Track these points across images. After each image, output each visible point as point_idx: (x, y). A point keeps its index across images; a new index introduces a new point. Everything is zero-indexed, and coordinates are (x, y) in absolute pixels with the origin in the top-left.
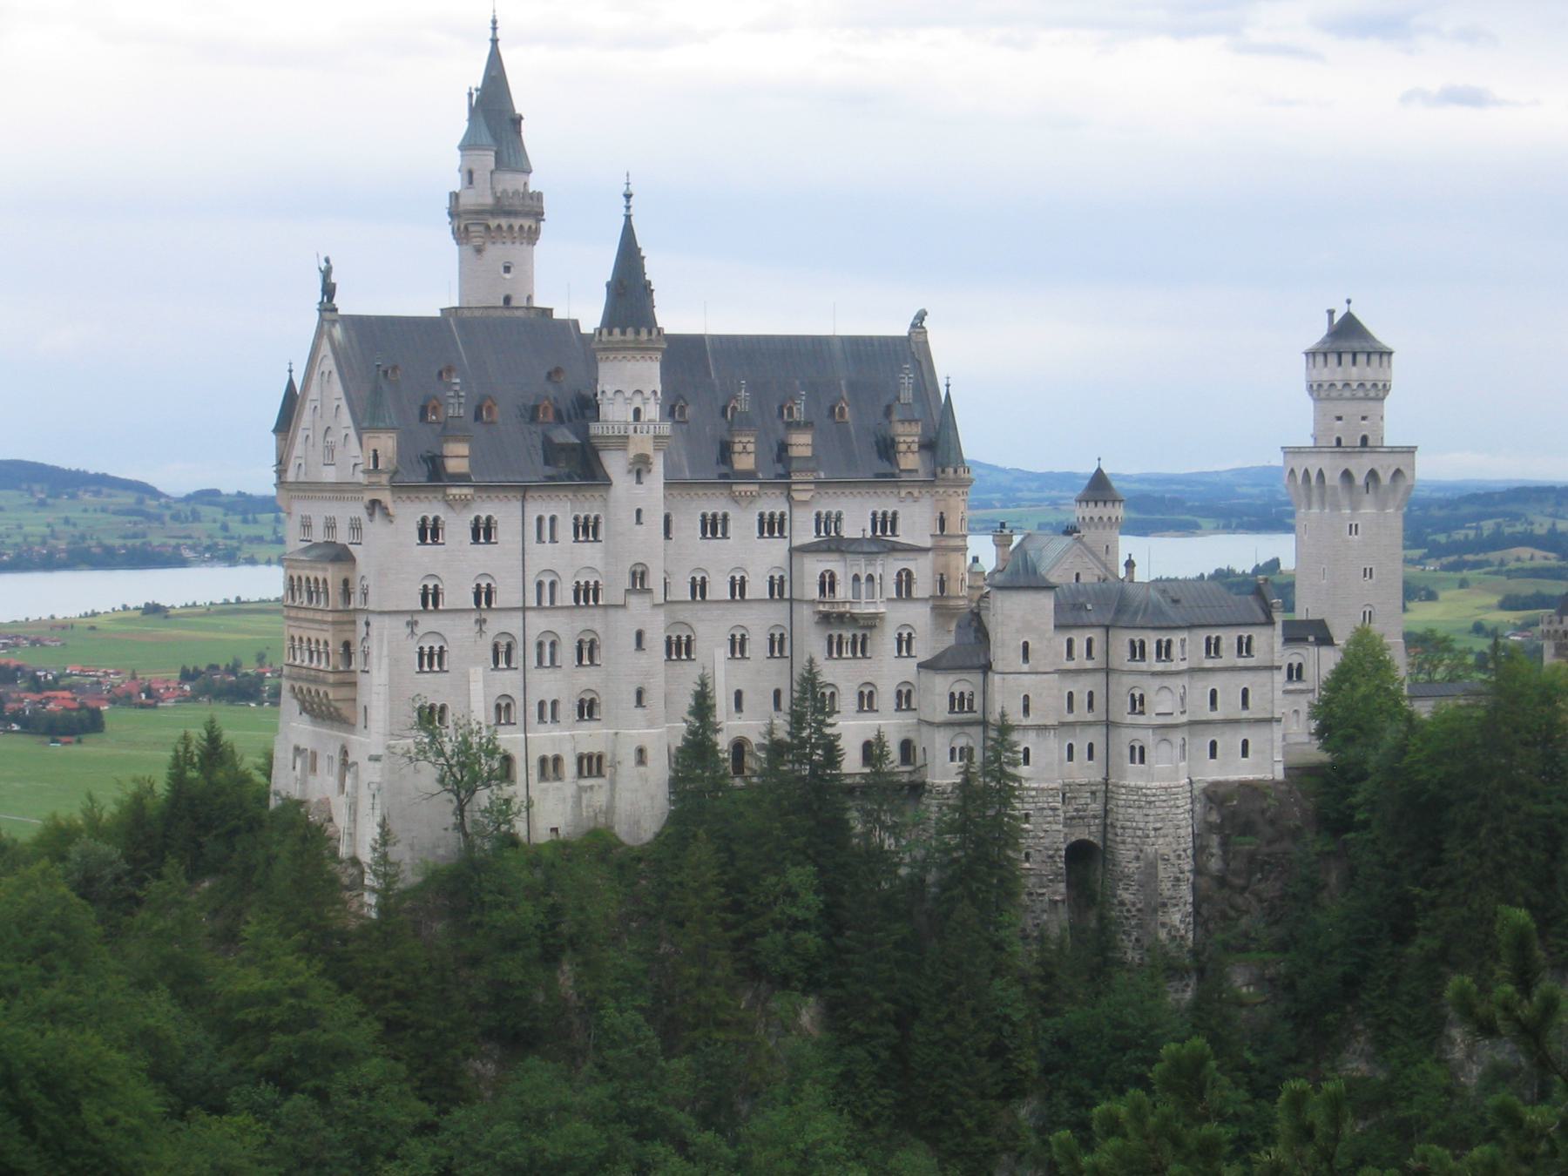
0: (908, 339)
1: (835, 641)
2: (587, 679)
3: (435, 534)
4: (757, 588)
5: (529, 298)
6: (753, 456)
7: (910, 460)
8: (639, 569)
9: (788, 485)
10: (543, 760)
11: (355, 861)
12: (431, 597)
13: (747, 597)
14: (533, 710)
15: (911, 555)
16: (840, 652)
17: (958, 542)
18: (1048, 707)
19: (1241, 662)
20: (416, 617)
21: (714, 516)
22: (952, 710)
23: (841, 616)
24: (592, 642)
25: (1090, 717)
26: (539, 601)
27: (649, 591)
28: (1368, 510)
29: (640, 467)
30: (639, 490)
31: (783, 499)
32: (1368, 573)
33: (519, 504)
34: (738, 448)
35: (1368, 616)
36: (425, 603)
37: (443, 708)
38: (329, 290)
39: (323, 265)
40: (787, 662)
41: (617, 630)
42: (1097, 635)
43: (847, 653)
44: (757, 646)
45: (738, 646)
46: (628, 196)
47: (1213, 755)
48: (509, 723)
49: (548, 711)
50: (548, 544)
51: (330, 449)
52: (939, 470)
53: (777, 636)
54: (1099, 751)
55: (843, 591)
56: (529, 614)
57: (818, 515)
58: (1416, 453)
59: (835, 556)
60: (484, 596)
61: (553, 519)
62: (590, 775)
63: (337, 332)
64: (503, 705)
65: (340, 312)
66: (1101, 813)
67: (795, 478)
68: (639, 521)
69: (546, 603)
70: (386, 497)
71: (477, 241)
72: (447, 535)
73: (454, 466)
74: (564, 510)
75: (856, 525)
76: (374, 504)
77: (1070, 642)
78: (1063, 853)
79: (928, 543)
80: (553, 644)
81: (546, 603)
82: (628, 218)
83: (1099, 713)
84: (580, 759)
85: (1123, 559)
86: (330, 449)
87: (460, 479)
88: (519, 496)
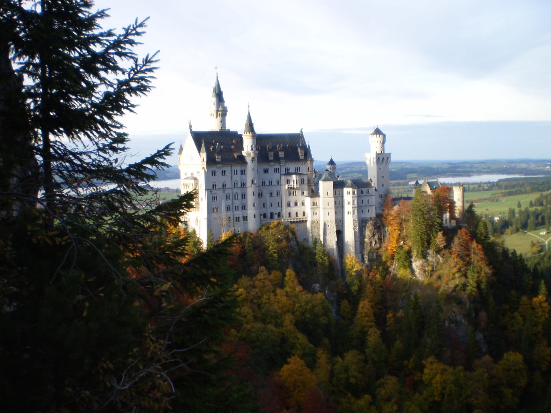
0: (299, 134)
1: (290, 192)
2: (244, 201)
3: (215, 175)
4: (274, 183)
5: (226, 128)
6: (273, 157)
7: (302, 157)
8: (253, 180)
9: (280, 163)
10: (236, 218)
11: (201, 239)
12: (214, 186)
13: (273, 184)
14: (234, 208)
15: (304, 175)
16: (291, 195)
17: (312, 173)
18: (332, 204)
19: (367, 194)
20: (212, 190)
21: (266, 169)
22: (313, 205)
23: (291, 188)
24: (244, 194)
25: (339, 206)
26: (235, 187)
27: (256, 184)
28: (383, 165)
29: (253, 159)
30: (253, 164)
31: (279, 165)
32: (383, 177)
33: (230, 167)
34: (270, 155)
35: (383, 185)
36: (213, 187)
37: (217, 208)
38: (191, 126)
39: (189, 122)
40: (280, 197)
41: (250, 191)
42: (340, 190)
43: (292, 195)
44: (275, 194)
45: (271, 194)
46: (249, 107)
47: (363, 212)
48: (229, 211)
49: (237, 208)
50: (236, 175)
51: (191, 159)
52: (308, 159)
53: (278, 192)
54: (341, 212)
55: (291, 183)
56: (233, 189)
57: (285, 168)
58: (391, 154)
59: (289, 176)
60: (224, 186)
61: (237, 170)
62: (245, 220)
63: (193, 134)
64: (228, 207)
65: (193, 131)
66: (342, 224)
67: (281, 161)
68: (253, 170)
69: (236, 187)
70: (205, 166)
71: (215, 116)
72: (217, 174)
73: (217, 160)
74: (238, 168)
75: (292, 170)
76: (203, 168)
77: (335, 192)
78: (335, 232)
79: (306, 173)
80: (237, 195)
81: (236, 187)
82: (249, 111)
83: (341, 205)
84: (243, 217)
85: (336, 175)
86: (191, 159)
87: (219, 163)
88: (230, 166)
